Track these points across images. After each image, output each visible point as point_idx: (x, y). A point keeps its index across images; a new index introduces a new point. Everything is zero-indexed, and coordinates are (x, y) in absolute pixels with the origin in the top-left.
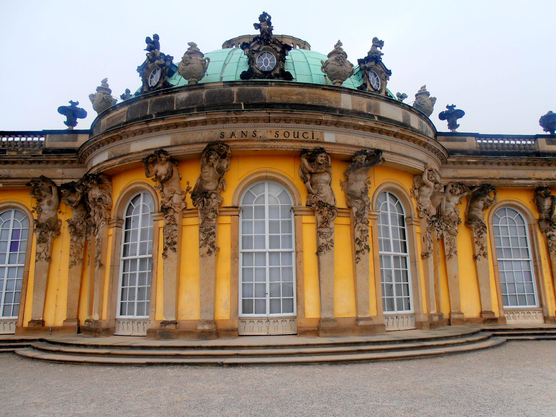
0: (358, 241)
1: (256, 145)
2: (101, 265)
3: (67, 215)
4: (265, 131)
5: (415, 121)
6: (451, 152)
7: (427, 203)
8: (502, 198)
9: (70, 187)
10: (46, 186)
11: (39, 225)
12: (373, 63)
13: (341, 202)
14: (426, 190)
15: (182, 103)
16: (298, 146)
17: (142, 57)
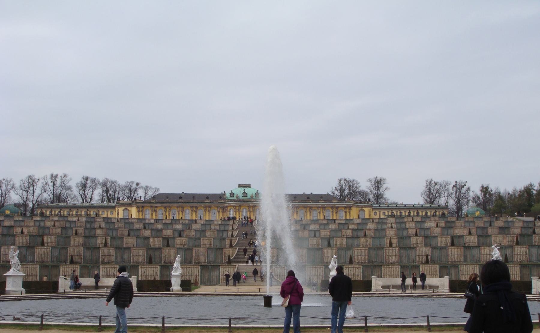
3: (221, 210)
17: (230, 192)
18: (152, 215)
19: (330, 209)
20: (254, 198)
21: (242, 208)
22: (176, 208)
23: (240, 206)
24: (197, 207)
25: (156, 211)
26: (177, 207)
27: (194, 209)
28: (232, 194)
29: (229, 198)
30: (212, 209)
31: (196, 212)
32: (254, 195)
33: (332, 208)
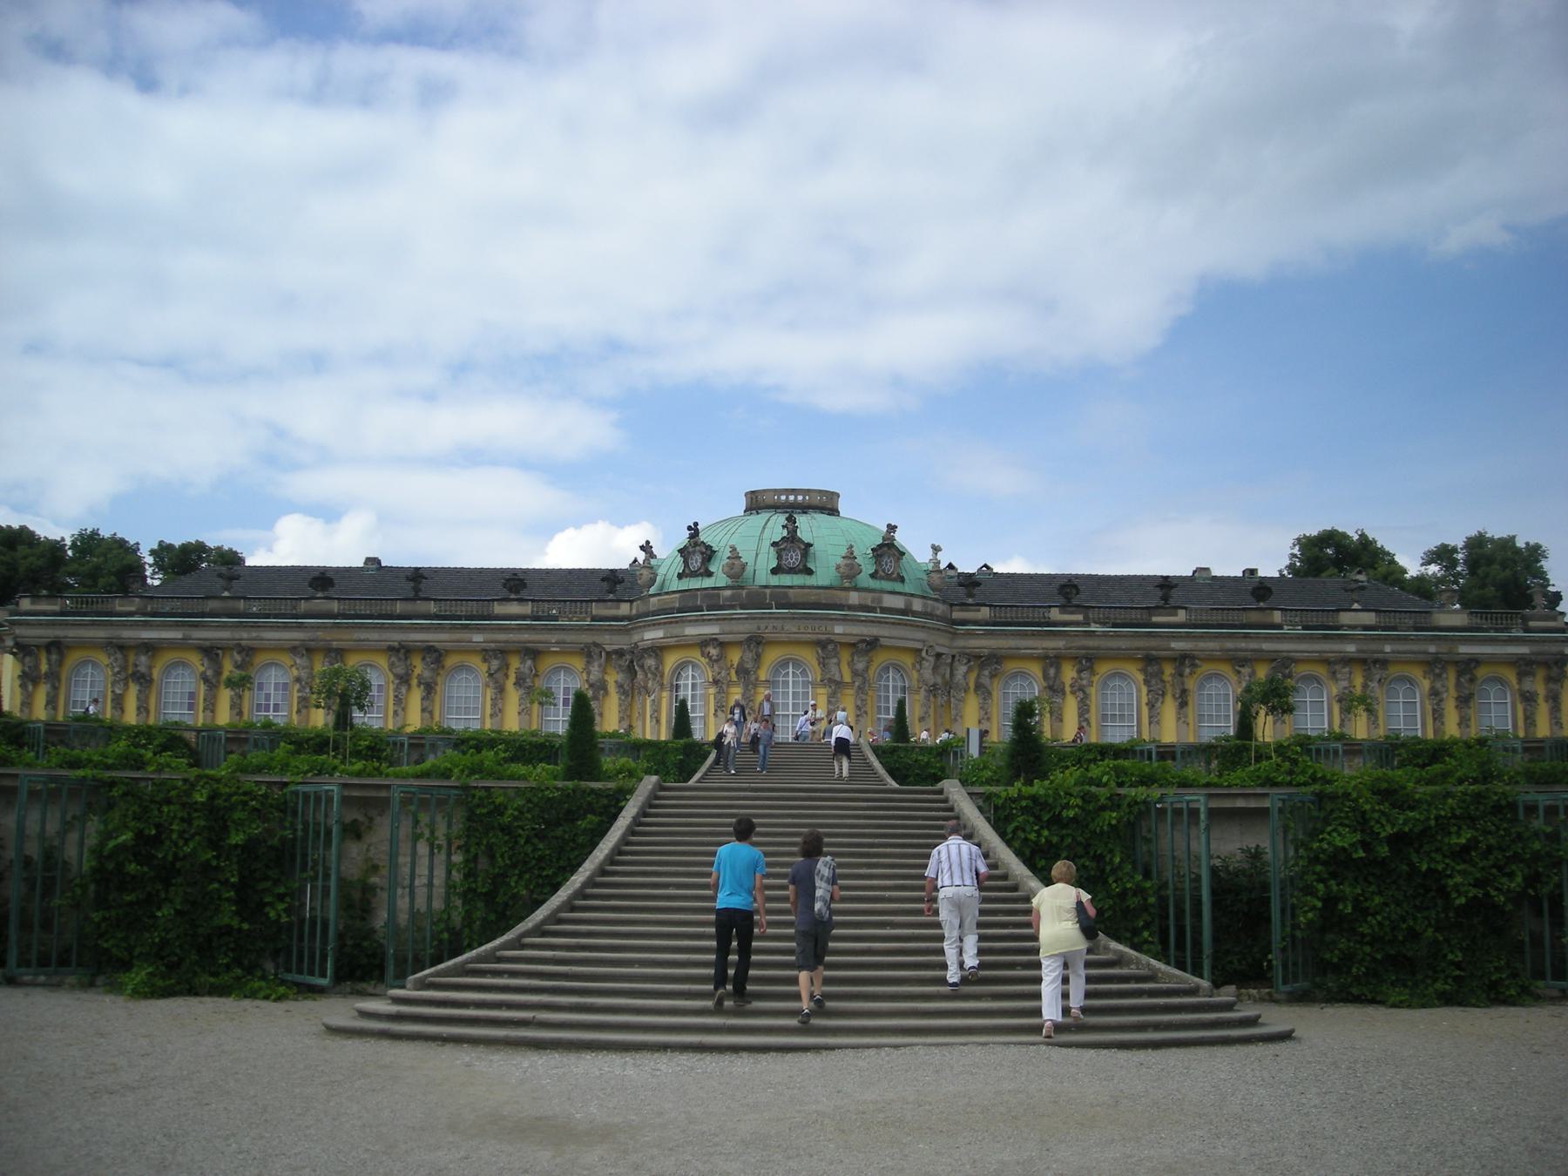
0: (858, 708)
1: (783, 637)
2: (658, 721)
3: (613, 678)
4: (790, 627)
5: (917, 605)
6: (964, 622)
7: (927, 673)
8: (1011, 666)
9: (620, 653)
10: (597, 650)
11: (591, 686)
12: (888, 549)
13: (847, 678)
14: (926, 664)
15: (726, 599)
16: (814, 637)
17: (683, 538)
18: (119, 702)
19: (1416, 673)
20: (864, 580)
21: (772, 656)
22: (286, 659)
23: (756, 642)
24: (435, 655)
25: (144, 680)
26: (294, 650)
27: (419, 667)
28: (696, 551)
29: (676, 585)
30: (547, 663)
31: (429, 688)
32: (868, 567)
33: (1434, 665)
